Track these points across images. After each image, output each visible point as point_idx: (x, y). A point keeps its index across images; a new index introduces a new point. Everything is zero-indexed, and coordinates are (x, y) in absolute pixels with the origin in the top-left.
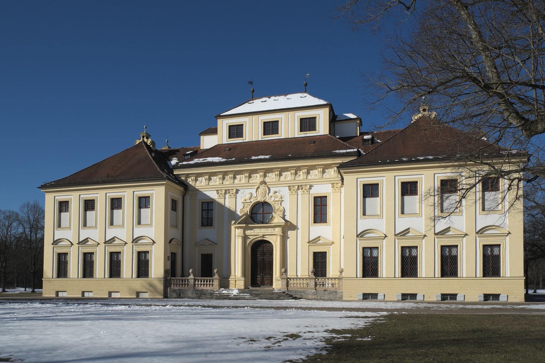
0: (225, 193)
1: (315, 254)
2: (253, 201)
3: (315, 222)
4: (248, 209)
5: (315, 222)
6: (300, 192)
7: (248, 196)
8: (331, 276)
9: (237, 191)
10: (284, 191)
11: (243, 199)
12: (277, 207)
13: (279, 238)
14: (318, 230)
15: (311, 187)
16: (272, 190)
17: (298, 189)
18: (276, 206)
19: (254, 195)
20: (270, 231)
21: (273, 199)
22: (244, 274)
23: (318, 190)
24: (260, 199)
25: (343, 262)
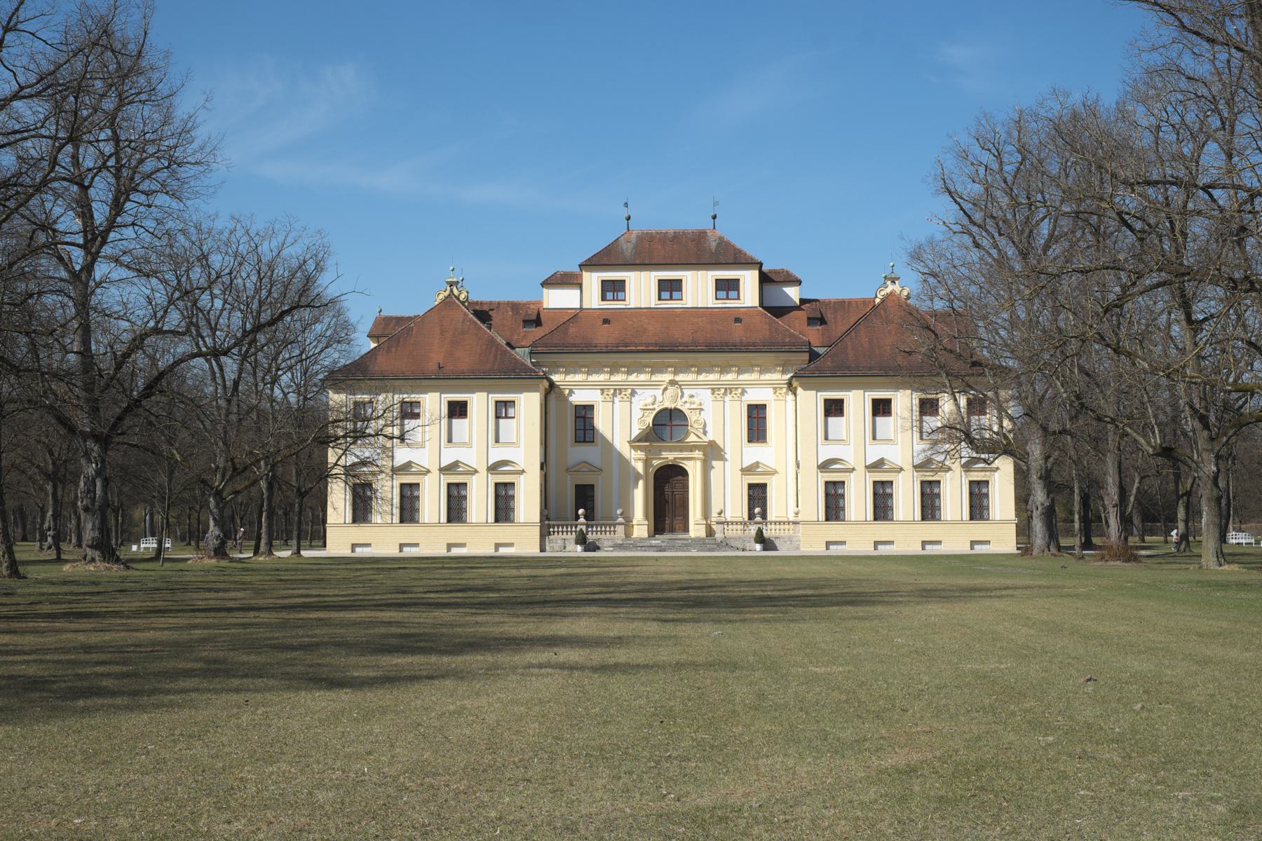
0: (614, 395)
1: (751, 486)
3: (749, 441)
4: (649, 420)
5: (749, 441)
6: (728, 398)
7: (650, 400)
8: (774, 519)
9: (633, 393)
10: (704, 396)
11: (642, 403)
12: (694, 418)
13: (699, 463)
14: (755, 453)
15: (743, 392)
16: (687, 392)
17: (725, 394)
18: (692, 417)
19: (660, 398)
21: (688, 406)
22: (646, 517)
23: (756, 396)
24: (668, 404)
25: (797, 500)
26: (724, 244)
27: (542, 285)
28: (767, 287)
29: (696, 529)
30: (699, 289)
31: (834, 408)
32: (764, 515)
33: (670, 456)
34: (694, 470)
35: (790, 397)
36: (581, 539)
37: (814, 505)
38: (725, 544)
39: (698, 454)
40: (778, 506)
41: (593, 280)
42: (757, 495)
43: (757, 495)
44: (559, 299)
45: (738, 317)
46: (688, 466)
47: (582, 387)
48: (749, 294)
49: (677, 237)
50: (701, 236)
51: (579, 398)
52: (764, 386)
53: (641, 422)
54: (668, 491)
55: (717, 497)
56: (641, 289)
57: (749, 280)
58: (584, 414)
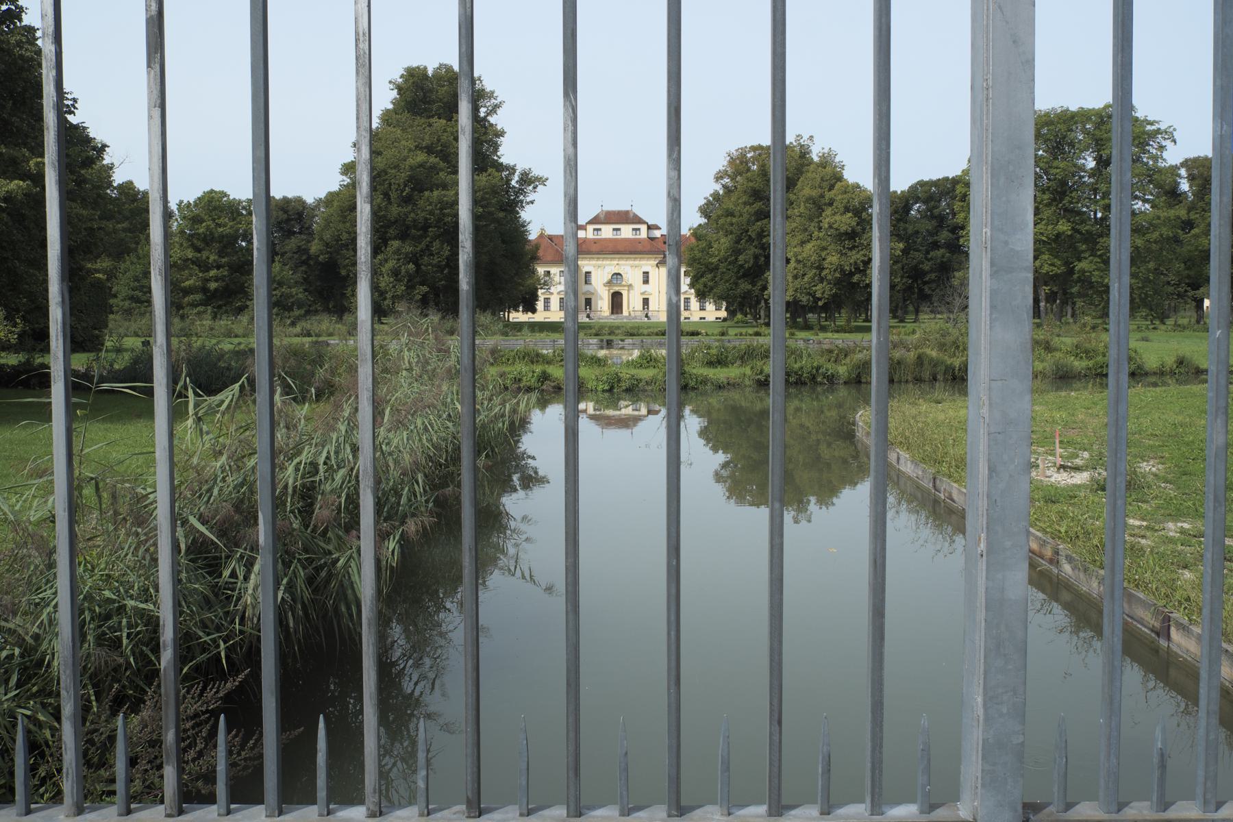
26: (636, 216)
29: (625, 313)
30: (626, 231)
33: (617, 289)
34: (625, 293)
36: (588, 316)
38: (635, 318)
40: (653, 306)
41: (590, 228)
42: (646, 302)
43: (646, 302)
45: (639, 241)
47: (586, 265)
48: (644, 233)
49: (619, 213)
50: (627, 212)
51: (585, 269)
52: (648, 264)
53: (607, 277)
54: (616, 301)
55: (633, 303)
56: (607, 231)
57: (644, 228)
58: (588, 274)
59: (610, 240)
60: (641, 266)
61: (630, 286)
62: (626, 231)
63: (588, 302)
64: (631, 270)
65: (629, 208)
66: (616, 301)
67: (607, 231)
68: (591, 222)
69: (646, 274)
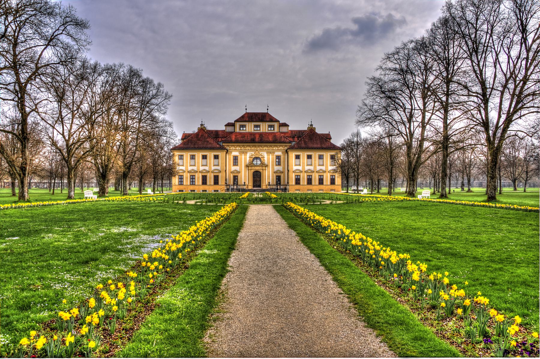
2: (253, 157)
10: (265, 154)
20: (260, 168)
27: (226, 126)
28: (281, 128)
30: (264, 128)
31: (298, 157)
32: (280, 184)
33: (257, 168)
35: (286, 155)
37: (293, 181)
39: (264, 168)
43: (278, 178)
44: (230, 129)
46: (261, 171)
54: (257, 177)
56: (250, 128)
57: (276, 125)
58: (236, 158)
59: (251, 134)
60: (274, 152)
61: (267, 166)
62: (264, 128)
63: (235, 178)
64: (268, 156)
65: (265, 111)
66: (257, 177)
67: (250, 128)
68: (237, 121)
69: (278, 157)
